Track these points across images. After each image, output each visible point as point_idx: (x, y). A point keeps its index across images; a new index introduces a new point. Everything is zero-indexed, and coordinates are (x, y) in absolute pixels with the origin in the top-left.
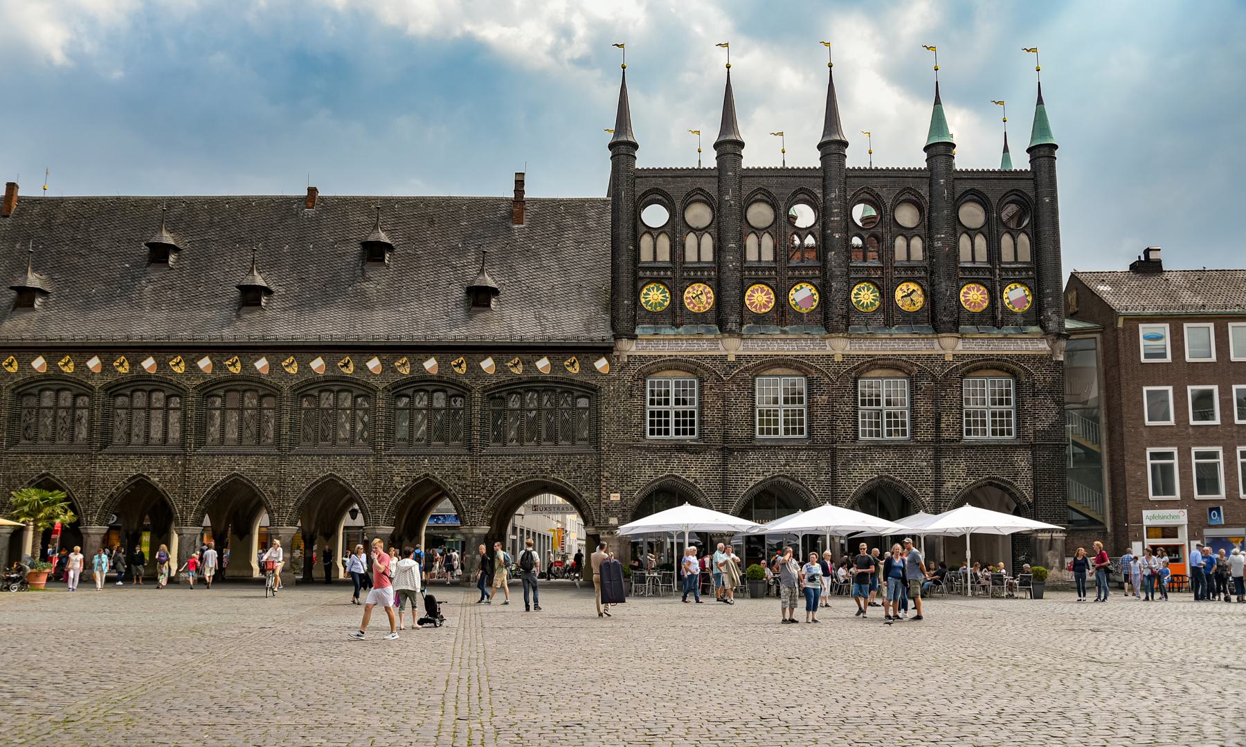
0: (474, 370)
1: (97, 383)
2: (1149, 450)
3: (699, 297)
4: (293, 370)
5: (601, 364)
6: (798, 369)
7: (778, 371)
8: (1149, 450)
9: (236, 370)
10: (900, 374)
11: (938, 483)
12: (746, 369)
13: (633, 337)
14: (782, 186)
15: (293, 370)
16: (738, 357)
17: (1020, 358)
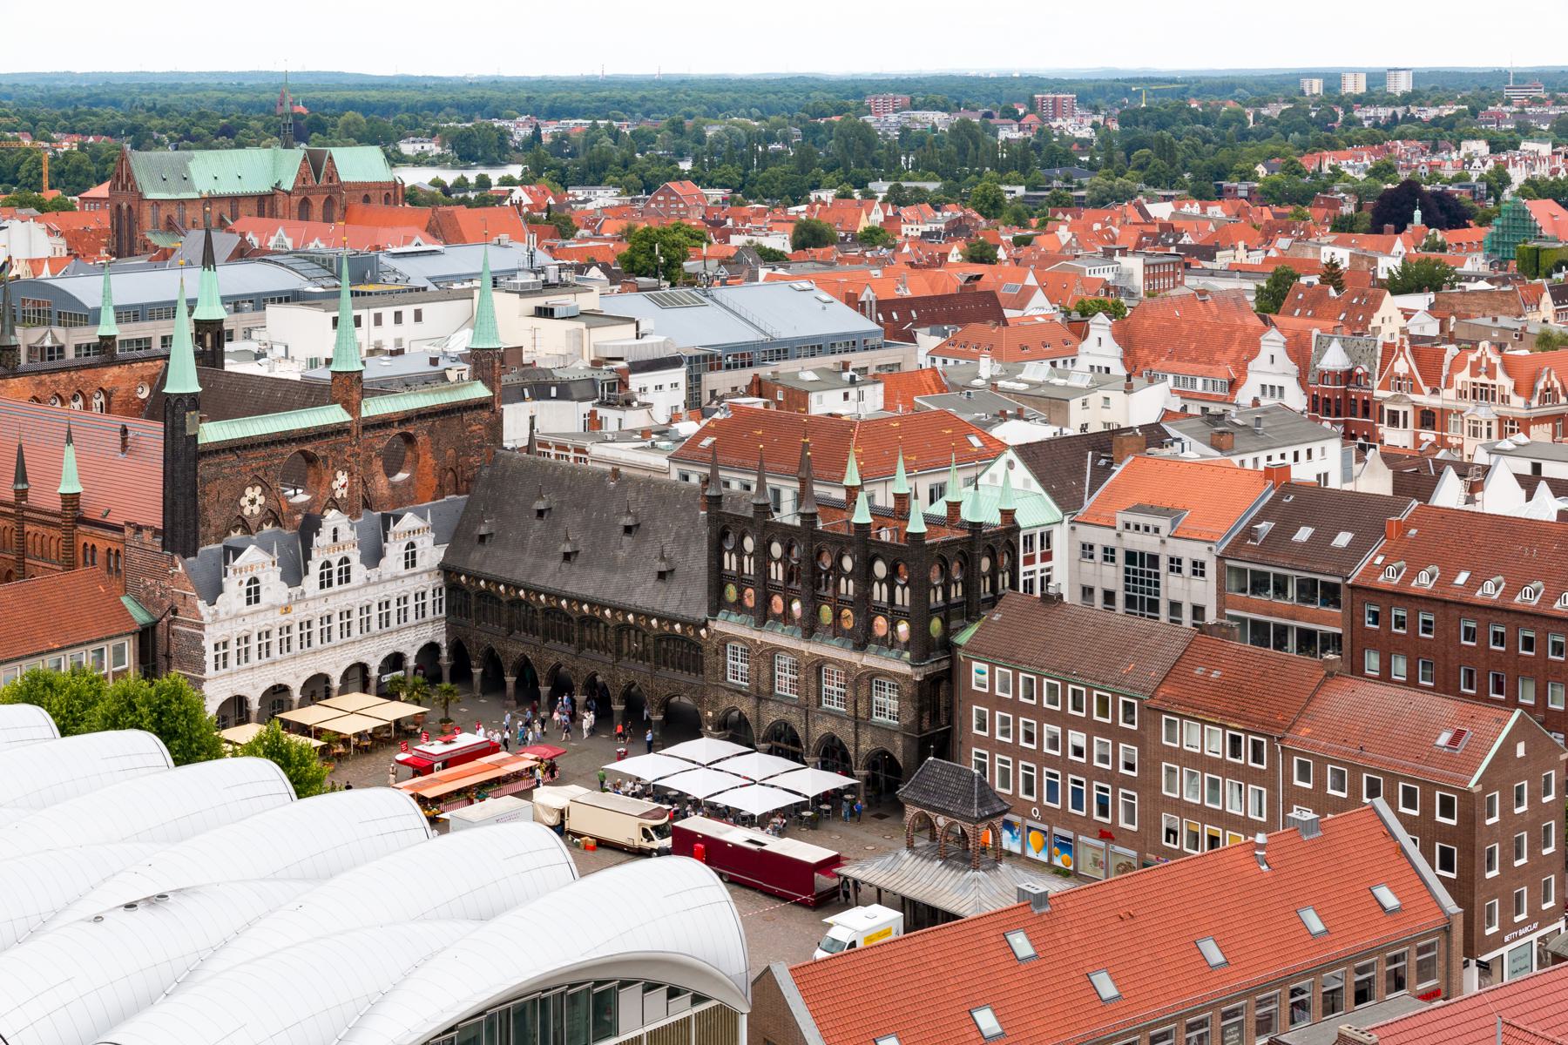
1: (504, 599)
5: (703, 632)
11: (857, 745)
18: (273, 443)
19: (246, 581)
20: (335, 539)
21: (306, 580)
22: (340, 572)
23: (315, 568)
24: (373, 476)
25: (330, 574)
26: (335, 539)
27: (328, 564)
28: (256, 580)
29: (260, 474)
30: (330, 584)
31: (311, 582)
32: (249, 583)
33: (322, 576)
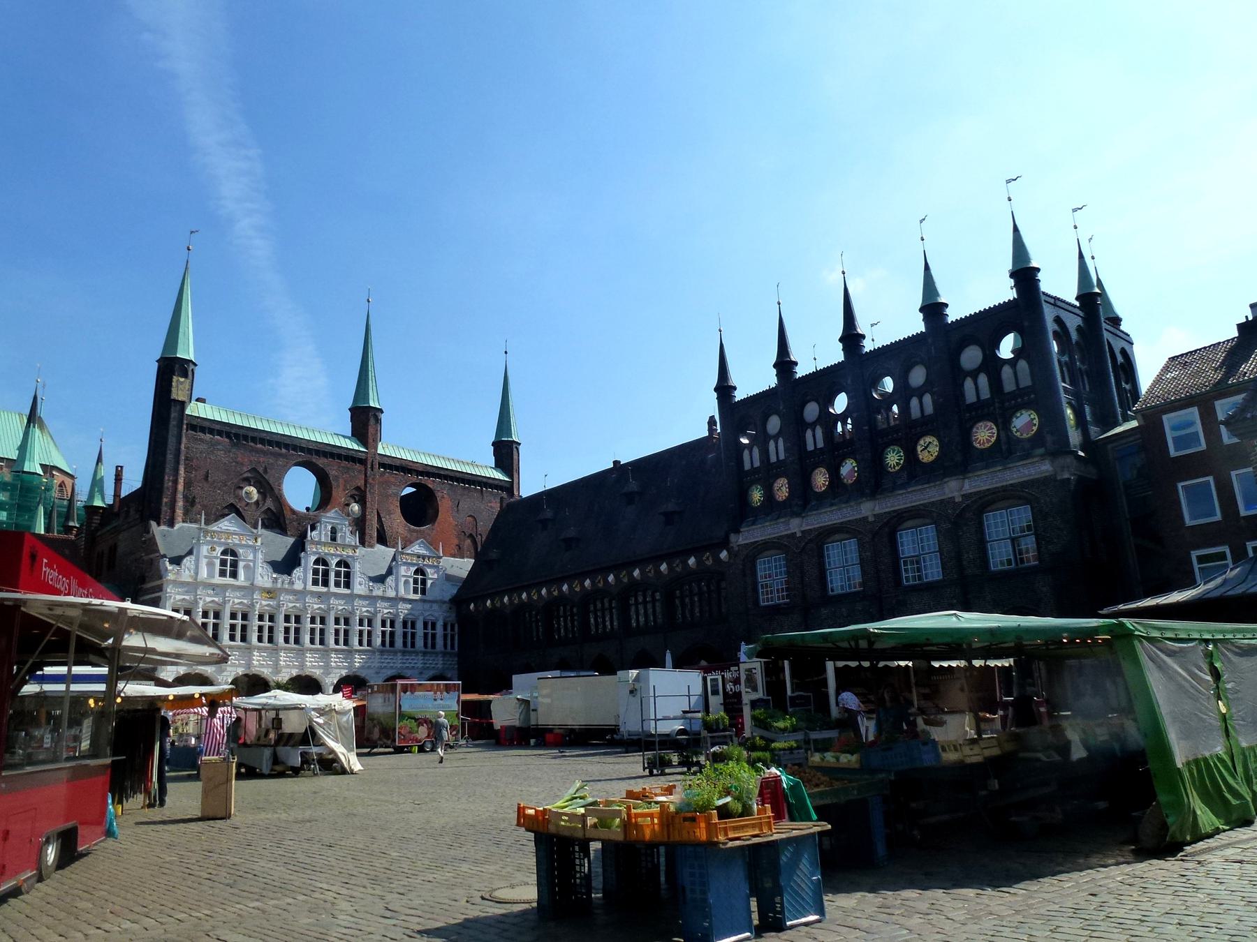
0: (658, 572)
2: (1194, 554)
3: (782, 489)
4: (578, 589)
5: (724, 555)
6: (847, 532)
7: (837, 537)
8: (1194, 554)
9: (556, 593)
10: (927, 521)
12: (811, 541)
13: (737, 531)
14: (826, 382)
15: (578, 589)
16: (803, 532)
17: (1024, 485)
18: (279, 444)
19: (219, 550)
20: (334, 539)
21: (297, 572)
22: (338, 574)
23: (309, 560)
24: (390, 513)
25: (326, 573)
26: (334, 539)
27: (325, 563)
28: (234, 554)
29: (261, 470)
30: (326, 583)
31: (302, 577)
32: (224, 553)
33: (316, 572)
